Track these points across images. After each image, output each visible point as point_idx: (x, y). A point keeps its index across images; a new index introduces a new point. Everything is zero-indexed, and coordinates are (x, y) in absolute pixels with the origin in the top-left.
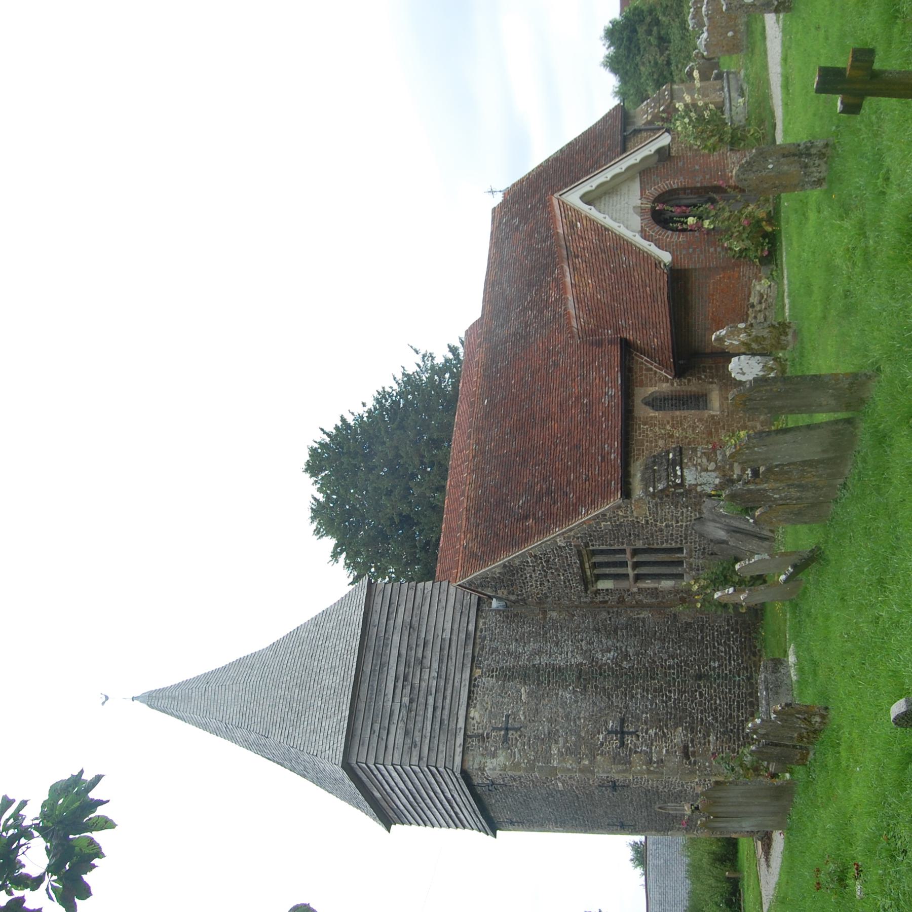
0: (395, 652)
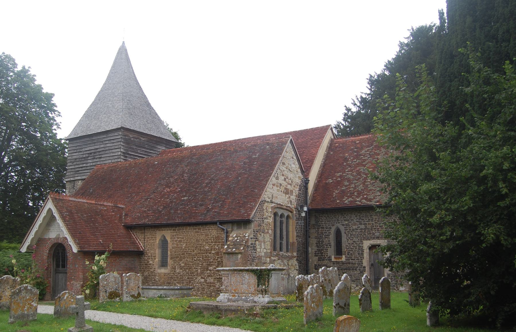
0: (98, 147)
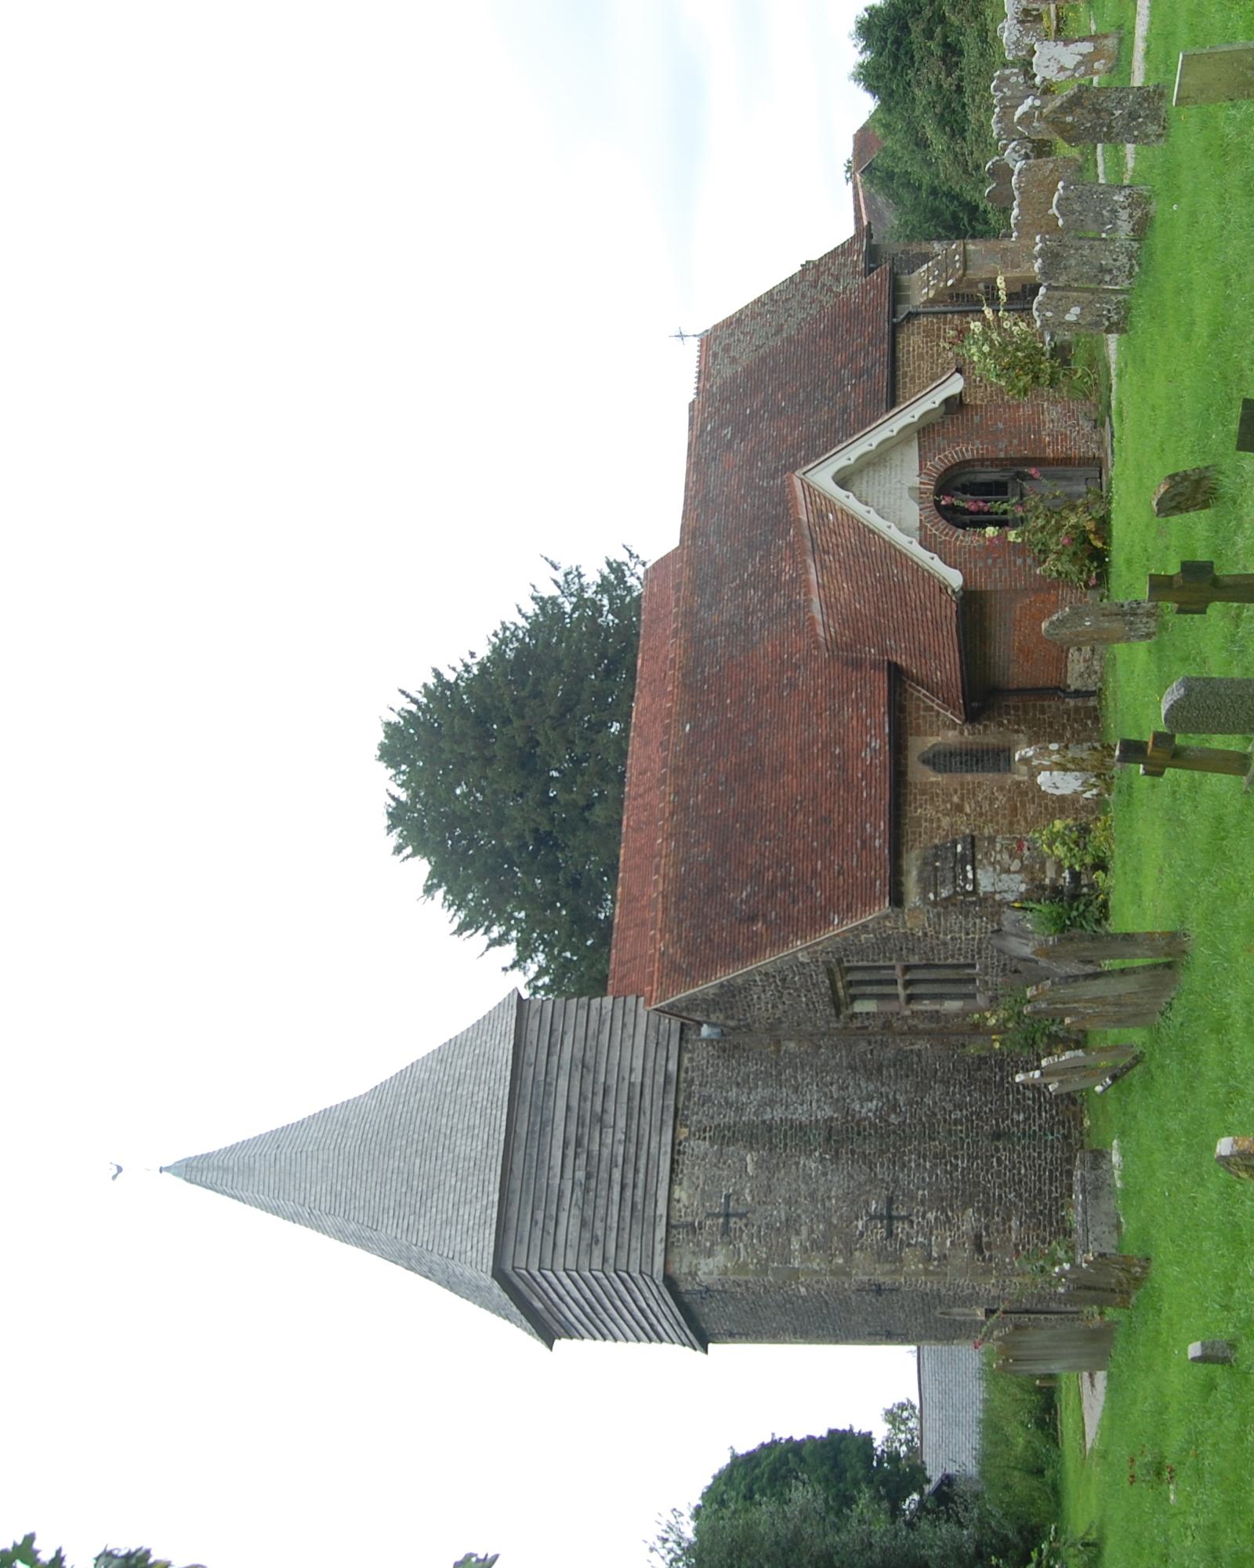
0: (561, 1104)
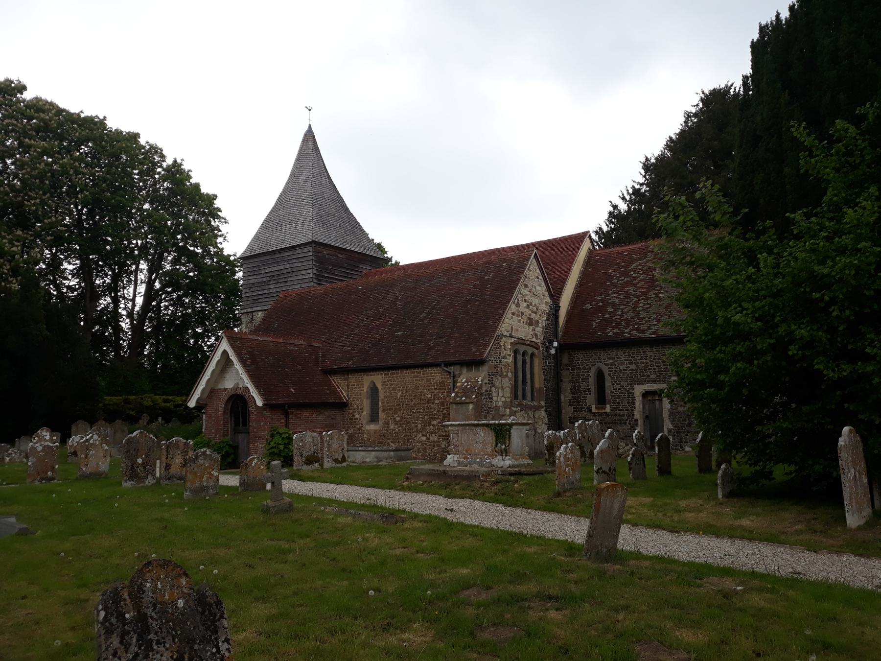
0: (282, 267)
